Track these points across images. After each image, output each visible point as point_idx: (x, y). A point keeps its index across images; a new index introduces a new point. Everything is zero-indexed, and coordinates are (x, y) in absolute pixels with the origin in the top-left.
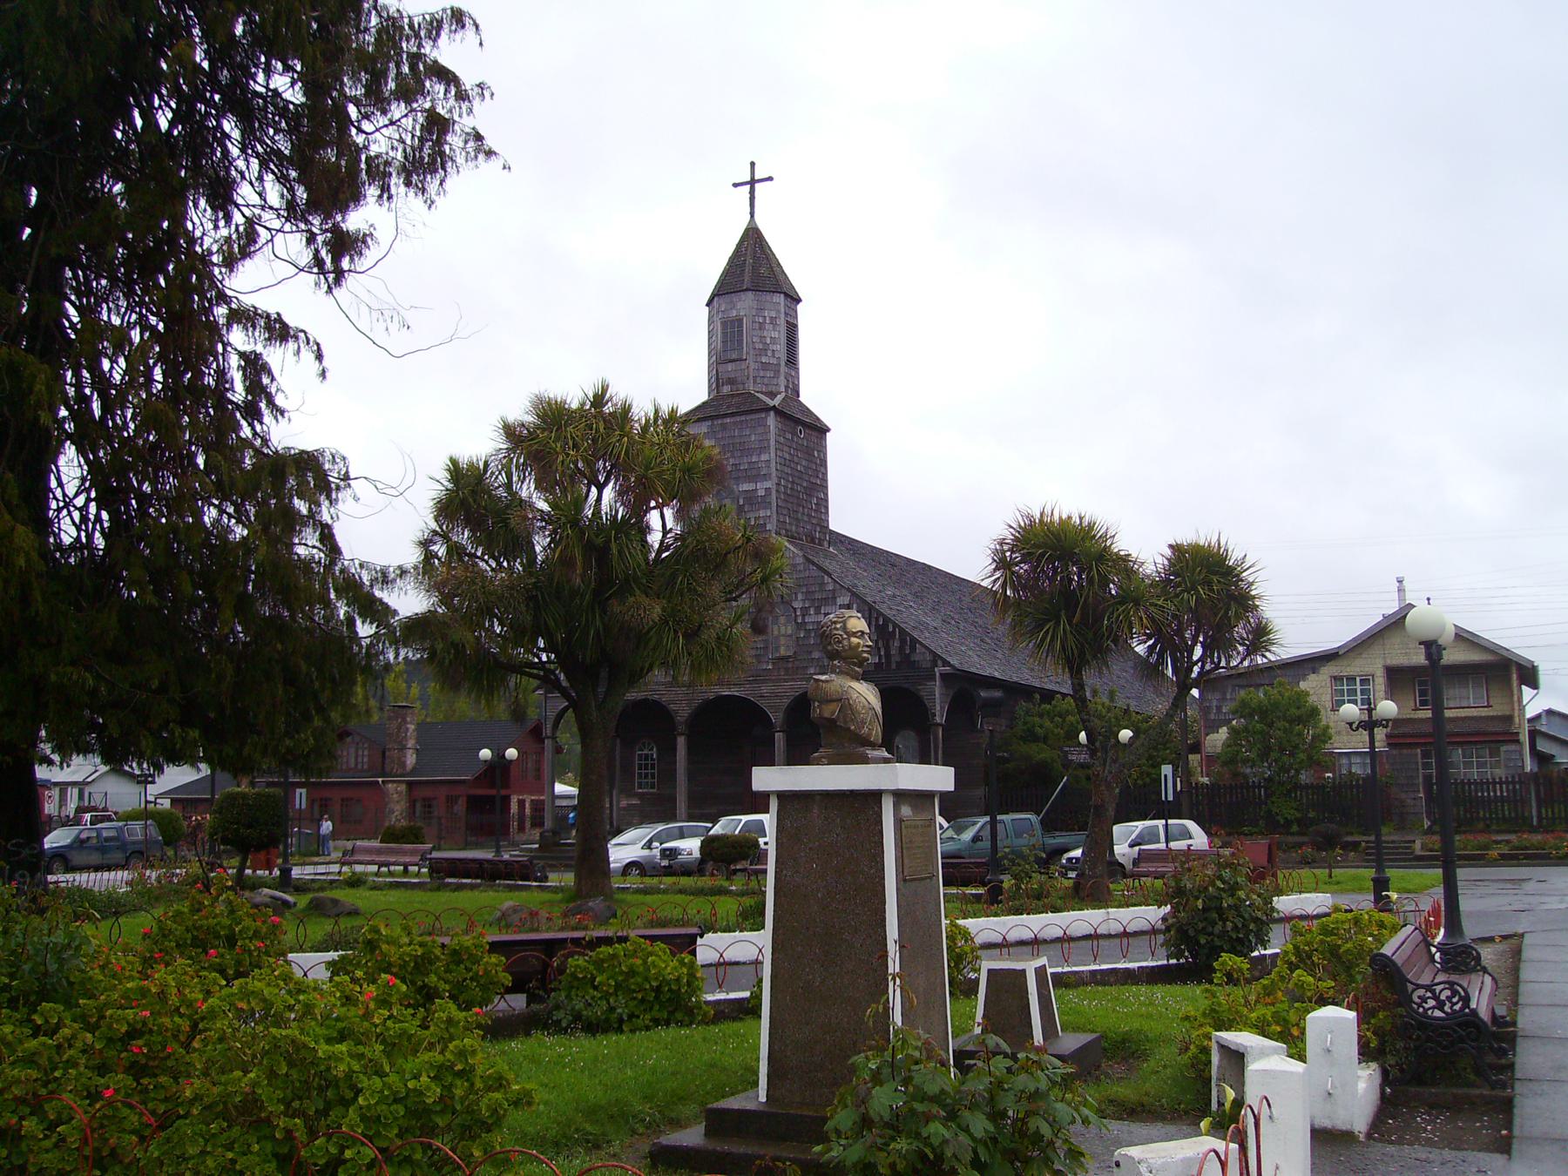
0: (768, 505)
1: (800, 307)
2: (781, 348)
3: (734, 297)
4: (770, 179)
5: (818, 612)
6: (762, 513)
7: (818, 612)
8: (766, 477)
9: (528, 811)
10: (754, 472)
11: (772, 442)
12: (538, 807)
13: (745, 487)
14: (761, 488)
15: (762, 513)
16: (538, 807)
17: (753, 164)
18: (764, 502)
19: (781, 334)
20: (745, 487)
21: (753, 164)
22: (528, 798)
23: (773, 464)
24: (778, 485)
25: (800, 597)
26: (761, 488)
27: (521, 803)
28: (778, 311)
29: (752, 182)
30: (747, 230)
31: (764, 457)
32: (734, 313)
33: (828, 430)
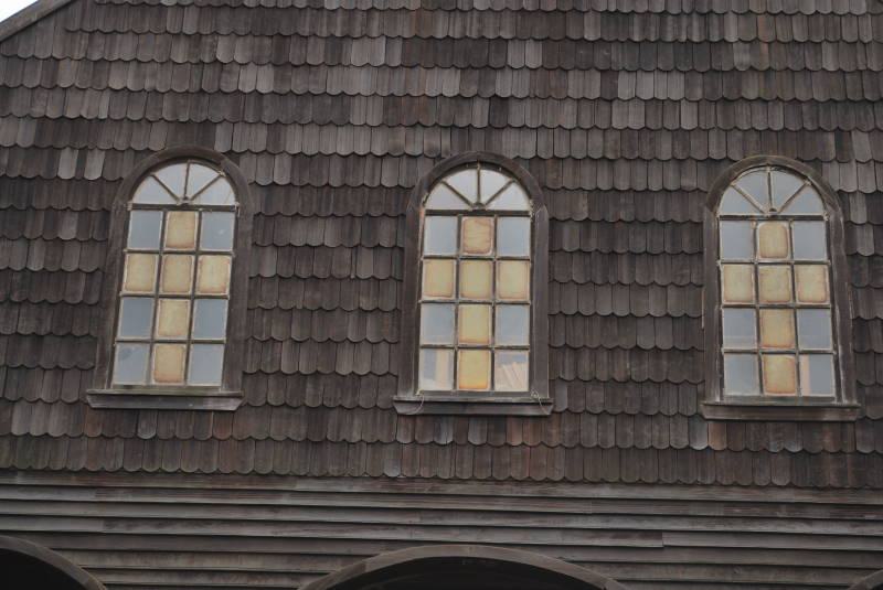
25: (862, 145)
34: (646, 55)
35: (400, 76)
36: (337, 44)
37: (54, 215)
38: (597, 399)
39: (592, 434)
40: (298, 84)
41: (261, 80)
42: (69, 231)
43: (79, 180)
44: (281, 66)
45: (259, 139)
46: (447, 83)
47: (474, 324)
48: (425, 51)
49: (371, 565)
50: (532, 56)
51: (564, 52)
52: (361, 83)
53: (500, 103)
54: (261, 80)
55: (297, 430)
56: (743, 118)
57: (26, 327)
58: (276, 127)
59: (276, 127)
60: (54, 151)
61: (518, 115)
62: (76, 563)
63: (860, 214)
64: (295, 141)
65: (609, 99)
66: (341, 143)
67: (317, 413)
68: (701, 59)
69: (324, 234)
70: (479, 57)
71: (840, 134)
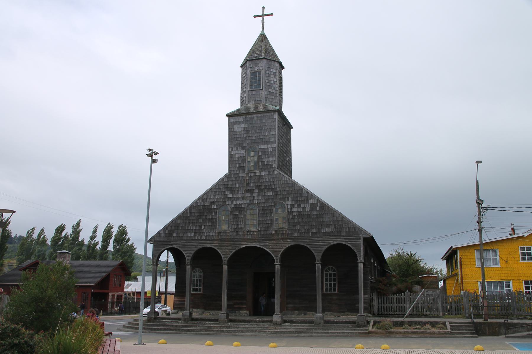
0: (273, 156)
1: (283, 71)
2: (277, 86)
3: (258, 62)
4: (272, 14)
5: (299, 206)
6: (271, 159)
7: (299, 206)
8: (273, 142)
9: (115, 300)
11: (277, 127)
12: (119, 297)
13: (263, 146)
14: (270, 147)
15: (271, 159)
16: (119, 297)
17: (264, 8)
18: (272, 154)
19: (277, 80)
20: (263, 146)
21: (264, 8)
22: (116, 294)
23: (277, 137)
24: (278, 146)
25: (290, 198)
26: (270, 147)
27: (113, 296)
28: (277, 69)
29: (263, 16)
30: (261, 35)
31: (273, 133)
32: (257, 68)
33: (292, 128)
34: (268, 190)
36: (238, 191)
37: (212, 212)
38: (263, 229)
39: (262, 233)
40: (235, 196)
41: (230, 196)
42: (213, 214)
44: (233, 194)
45: (230, 202)
46: (248, 195)
48: (247, 191)
50: (257, 191)
51: (260, 190)
52: (240, 196)
53: (254, 197)
54: (230, 196)
57: (210, 224)
58: (232, 201)
59: (232, 201)
62: (215, 248)
63: (289, 207)
64: (234, 202)
65: (265, 195)
66: (239, 202)
67: (237, 232)
68: (273, 189)
69: (237, 213)
70: (251, 191)
71: (288, 198)
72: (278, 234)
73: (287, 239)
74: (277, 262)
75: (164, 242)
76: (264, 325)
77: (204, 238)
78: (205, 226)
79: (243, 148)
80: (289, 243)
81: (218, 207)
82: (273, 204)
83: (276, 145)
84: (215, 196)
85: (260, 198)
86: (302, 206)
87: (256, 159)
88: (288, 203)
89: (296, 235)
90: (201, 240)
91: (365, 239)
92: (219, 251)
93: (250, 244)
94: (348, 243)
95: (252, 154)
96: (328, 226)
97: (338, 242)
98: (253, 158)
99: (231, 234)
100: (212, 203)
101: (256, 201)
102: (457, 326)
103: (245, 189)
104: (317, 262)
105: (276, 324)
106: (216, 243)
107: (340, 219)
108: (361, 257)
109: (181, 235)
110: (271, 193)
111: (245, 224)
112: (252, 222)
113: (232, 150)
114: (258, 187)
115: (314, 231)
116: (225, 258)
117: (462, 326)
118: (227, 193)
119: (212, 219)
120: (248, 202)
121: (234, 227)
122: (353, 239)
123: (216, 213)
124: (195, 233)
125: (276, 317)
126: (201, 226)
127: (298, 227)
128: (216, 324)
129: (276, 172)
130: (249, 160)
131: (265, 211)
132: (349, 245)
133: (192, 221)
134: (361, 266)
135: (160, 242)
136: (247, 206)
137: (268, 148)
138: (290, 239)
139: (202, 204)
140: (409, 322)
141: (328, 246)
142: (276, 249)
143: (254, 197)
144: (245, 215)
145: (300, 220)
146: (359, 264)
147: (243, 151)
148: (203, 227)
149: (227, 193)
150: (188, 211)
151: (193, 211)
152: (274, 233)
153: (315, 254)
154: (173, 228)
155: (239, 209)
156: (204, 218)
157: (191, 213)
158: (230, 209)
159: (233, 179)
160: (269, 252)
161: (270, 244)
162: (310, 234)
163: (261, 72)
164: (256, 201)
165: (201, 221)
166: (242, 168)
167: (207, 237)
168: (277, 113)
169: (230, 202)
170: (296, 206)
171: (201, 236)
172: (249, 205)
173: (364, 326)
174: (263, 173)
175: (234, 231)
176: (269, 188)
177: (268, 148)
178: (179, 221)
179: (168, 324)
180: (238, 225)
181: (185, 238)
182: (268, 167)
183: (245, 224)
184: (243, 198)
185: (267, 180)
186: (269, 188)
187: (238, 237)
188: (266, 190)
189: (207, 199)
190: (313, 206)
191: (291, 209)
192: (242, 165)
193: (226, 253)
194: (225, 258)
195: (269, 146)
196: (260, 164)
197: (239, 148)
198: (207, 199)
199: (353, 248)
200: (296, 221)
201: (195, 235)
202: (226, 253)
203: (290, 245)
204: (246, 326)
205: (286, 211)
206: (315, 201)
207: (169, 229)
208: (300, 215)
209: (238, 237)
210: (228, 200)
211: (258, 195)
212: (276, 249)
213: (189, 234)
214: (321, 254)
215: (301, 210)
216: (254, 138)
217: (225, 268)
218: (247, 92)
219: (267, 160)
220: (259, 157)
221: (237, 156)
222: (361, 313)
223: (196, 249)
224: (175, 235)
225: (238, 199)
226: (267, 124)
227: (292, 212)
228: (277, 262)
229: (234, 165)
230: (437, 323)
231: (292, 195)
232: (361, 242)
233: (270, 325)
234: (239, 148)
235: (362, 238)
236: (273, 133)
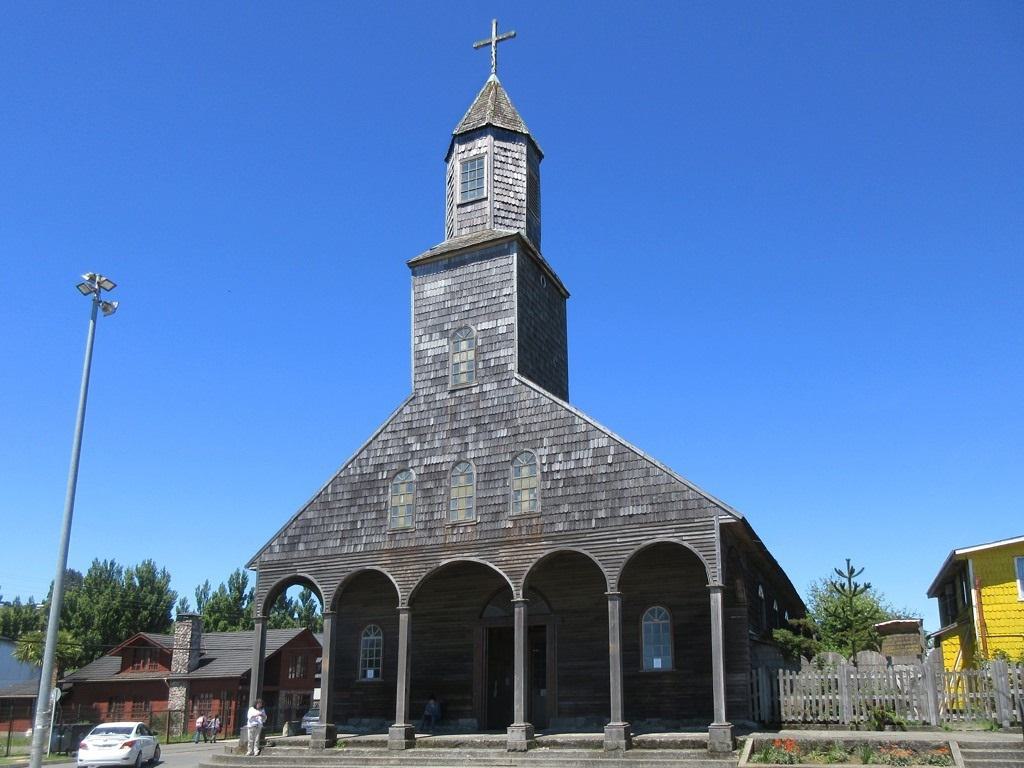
5: (569, 452)
6: (503, 353)
10: (494, 309)
15: (503, 353)
18: (504, 339)
20: (485, 325)
25: (546, 442)
32: (474, 152)
35: (446, 441)
38: (486, 518)
39: (485, 527)
40: (426, 446)
42: (381, 492)
43: (382, 479)
46: (454, 441)
47: (462, 504)
48: (454, 432)
49: (441, 565)
50: (473, 430)
52: (437, 444)
53: (467, 443)
55: (426, 534)
56: (520, 439)
57: (374, 516)
60: (377, 472)
61: (471, 447)
62: (384, 570)
64: (426, 461)
66: (434, 460)
67: (431, 529)
72: (520, 528)
73: (538, 540)
74: (518, 596)
75: (280, 564)
76: (487, 755)
77: (360, 548)
78: (363, 521)
79: (444, 333)
80: (543, 550)
81: (391, 475)
82: (508, 458)
83: (513, 319)
84: (384, 449)
85: (481, 446)
86: (573, 458)
87: (471, 355)
88: (541, 451)
89: (560, 527)
90: (355, 553)
91: (725, 529)
92: (391, 578)
93: (459, 557)
94: (686, 540)
95: (464, 345)
96: (636, 500)
97: (660, 539)
98: (465, 355)
99: (417, 534)
100: (380, 467)
101: (470, 455)
102: (983, 755)
103: (448, 427)
104: (609, 592)
105: (514, 750)
106: (386, 559)
107: (663, 480)
108: (715, 576)
109: (314, 546)
110: (504, 433)
111: (448, 509)
112: (462, 501)
113: (420, 342)
114: (477, 421)
115: (602, 514)
116: (403, 595)
117: (997, 755)
118: (411, 440)
119: (379, 503)
120: (455, 457)
121: (423, 517)
122: (697, 529)
123: (386, 488)
124: (343, 538)
125: (516, 734)
126: (354, 522)
127: (565, 508)
128: (380, 753)
129: (514, 382)
130: (456, 360)
131: (490, 476)
132: (685, 544)
133: (336, 512)
134: (717, 599)
135: (269, 565)
136: (453, 468)
137: (497, 327)
138: (547, 539)
139: (358, 472)
140: (847, 742)
141: (637, 548)
142: (513, 566)
143: (467, 443)
144: (448, 490)
145: (570, 490)
146: (713, 595)
147: (444, 342)
148: (359, 525)
149: (411, 440)
150: (329, 490)
151: (340, 489)
152: (510, 525)
153: (604, 570)
154: (298, 532)
155: (435, 475)
156: (362, 501)
157: (335, 493)
158: (414, 477)
159: (423, 408)
160: (501, 572)
161: (503, 553)
162: (594, 521)
163: (483, 158)
164: (470, 455)
165: (354, 510)
166: (439, 381)
167: (366, 549)
168: (515, 243)
169: (416, 463)
170: (560, 457)
171: (356, 545)
172: (457, 463)
173: (726, 754)
174: (487, 388)
175: (425, 529)
176: (499, 419)
177: (497, 327)
178: (310, 515)
179: (280, 755)
180: (432, 513)
181: (321, 552)
182: (498, 372)
183: (448, 509)
184: (444, 450)
185: (496, 403)
186: (499, 419)
187: (431, 542)
188: (492, 427)
189: (367, 459)
190: (599, 454)
191: (550, 464)
192: (441, 373)
193: (403, 583)
194: (403, 595)
195: (499, 321)
196: (481, 365)
197: (436, 336)
198: (367, 459)
199: (696, 551)
200: (560, 492)
201: (342, 546)
202: (403, 583)
203: (547, 552)
204: (447, 757)
205: (539, 473)
206: (604, 442)
207: (290, 532)
208: (570, 481)
209: (431, 542)
210: (412, 458)
211: (476, 441)
212: (513, 566)
213: (331, 544)
214: (617, 571)
215: (572, 465)
216: (467, 308)
217: (404, 618)
218: (455, 208)
219: (494, 355)
220: (479, 352)
221: (430, 353)
222: (721, 721)
223: (343, 576)
224: (301, 547)
225: (432, 452)
226: (494, 271)
227: (552, 472)
228: (518, 596)
229: (424, 376)
230: (925, 745)
231: (551, 433)
232: (716, 535)
233: (501, 754)
234: (436, 336)
235: (717, 525)
236: (506, 291)
